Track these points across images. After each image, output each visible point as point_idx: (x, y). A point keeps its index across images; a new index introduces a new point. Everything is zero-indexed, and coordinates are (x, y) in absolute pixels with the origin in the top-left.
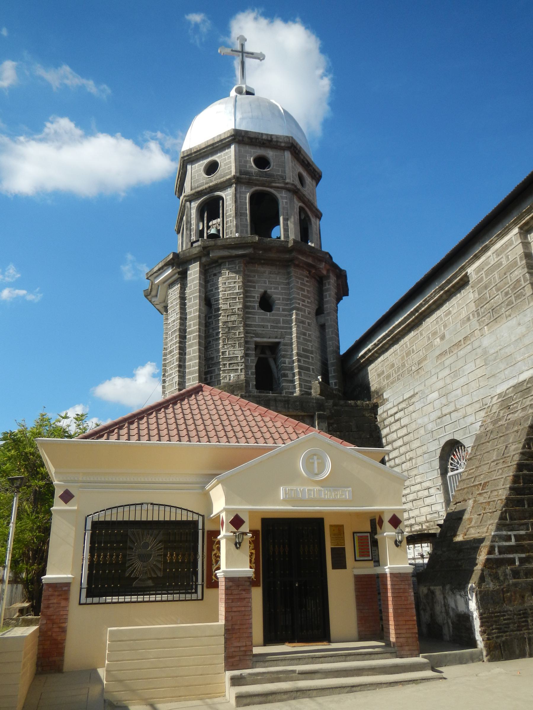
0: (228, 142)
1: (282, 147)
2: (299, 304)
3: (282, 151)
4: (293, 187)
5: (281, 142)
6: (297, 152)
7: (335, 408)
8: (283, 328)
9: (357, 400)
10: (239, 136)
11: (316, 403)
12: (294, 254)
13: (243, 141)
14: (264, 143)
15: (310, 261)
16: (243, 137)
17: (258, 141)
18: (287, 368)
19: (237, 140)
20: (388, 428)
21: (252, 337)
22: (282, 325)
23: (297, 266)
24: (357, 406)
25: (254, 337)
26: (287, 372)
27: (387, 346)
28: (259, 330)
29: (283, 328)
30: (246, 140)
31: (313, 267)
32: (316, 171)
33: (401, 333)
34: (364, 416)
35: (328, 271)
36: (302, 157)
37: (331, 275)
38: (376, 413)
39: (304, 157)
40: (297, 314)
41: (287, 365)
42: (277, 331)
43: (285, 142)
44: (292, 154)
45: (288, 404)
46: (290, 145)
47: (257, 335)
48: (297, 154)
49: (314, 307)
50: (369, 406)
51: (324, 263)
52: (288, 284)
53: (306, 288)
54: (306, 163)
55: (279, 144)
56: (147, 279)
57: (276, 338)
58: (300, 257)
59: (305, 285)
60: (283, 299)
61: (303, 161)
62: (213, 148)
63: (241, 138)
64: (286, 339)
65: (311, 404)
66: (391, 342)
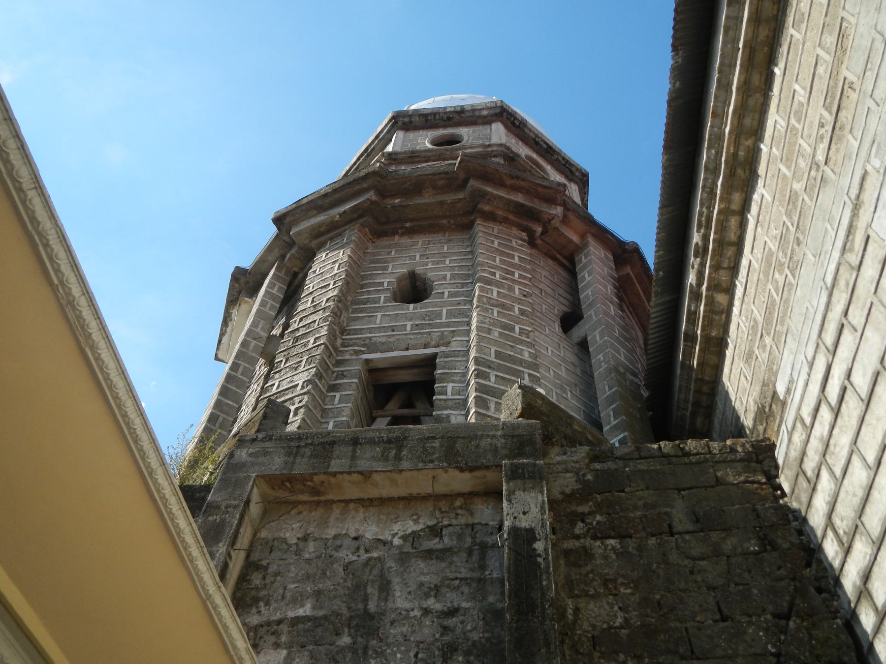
0: (387, 132)
1: (485, 117)
2: (494, 274)
3: (487, 127)
4: (500, 149)
5: (480, 109)
6: (517, 123)
7: (598, 466)
8: (448, 325)
9: (683, 437)
10: (404, 117)
11: (504, 436)
12: (473, 183)
13: (411, 122)
14: (449, 119)
15: (520, 198)
16: (410, 116)
17: (437, 117)
18: (450, 403)
19: (400, 123)
20: (825, 474)
21: (357, 353)
22: (444, 319)
23: (490, 217)
24: (688, 454)
25: (363, 352)
26: (446, 412)
27: (734, 221)
28: (379, 337)
29: (448, 325)
30: (416, 119)
31: (532, 215)
32: (571, 165)
33: (747, 121)
34: (718, 482)
35: (583, 236)
36: (531, 135)
37: (591, 240)
38: (771, 471)
39: (537, 136)
40: (482, 289)
41: (449, 395)
42: (429, 333)
43: (488, 108)
44: (506, 127)
45: (400, 449)
46: (498, 111)
47: (372, 347)
48: (519, 127)
49: (560, 307)
50: (733, 450)
51: (559, 210)
52: (472, 252)
53: (516, 254)
54: (545, 146)
55: (477, 113)
56: (217, 358)
57: (426, 346)
58: (489, 189)
59: (513, 249)
60: (453, 277)
61: (537, 143)
62: (368, 156)
63: (406, 120)
64: (453, 344)
65: (485, 443)
66: (737, 197)
